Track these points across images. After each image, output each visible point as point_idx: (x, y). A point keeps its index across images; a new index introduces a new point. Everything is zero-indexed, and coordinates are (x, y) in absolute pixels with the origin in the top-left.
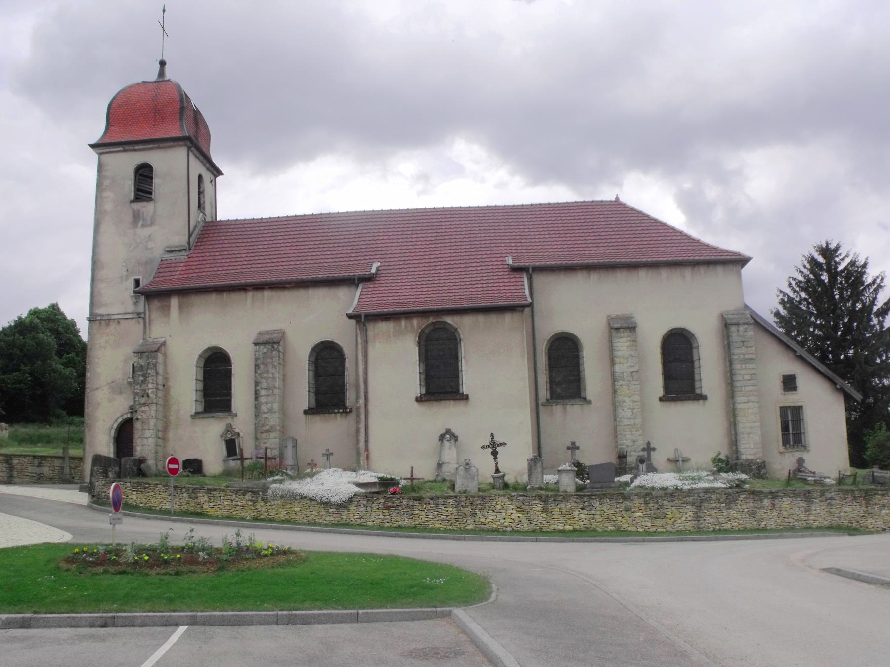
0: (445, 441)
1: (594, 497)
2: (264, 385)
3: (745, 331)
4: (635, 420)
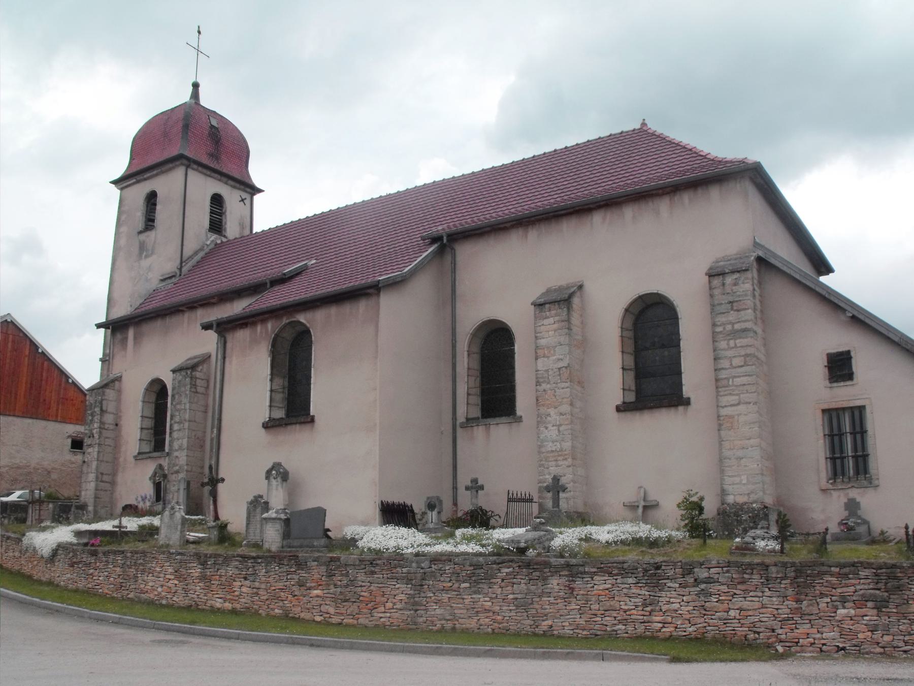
0: (272, 478)
1: (260, 561)
2: (177, 419)
3: (735, 284)
4: (563, 443)
